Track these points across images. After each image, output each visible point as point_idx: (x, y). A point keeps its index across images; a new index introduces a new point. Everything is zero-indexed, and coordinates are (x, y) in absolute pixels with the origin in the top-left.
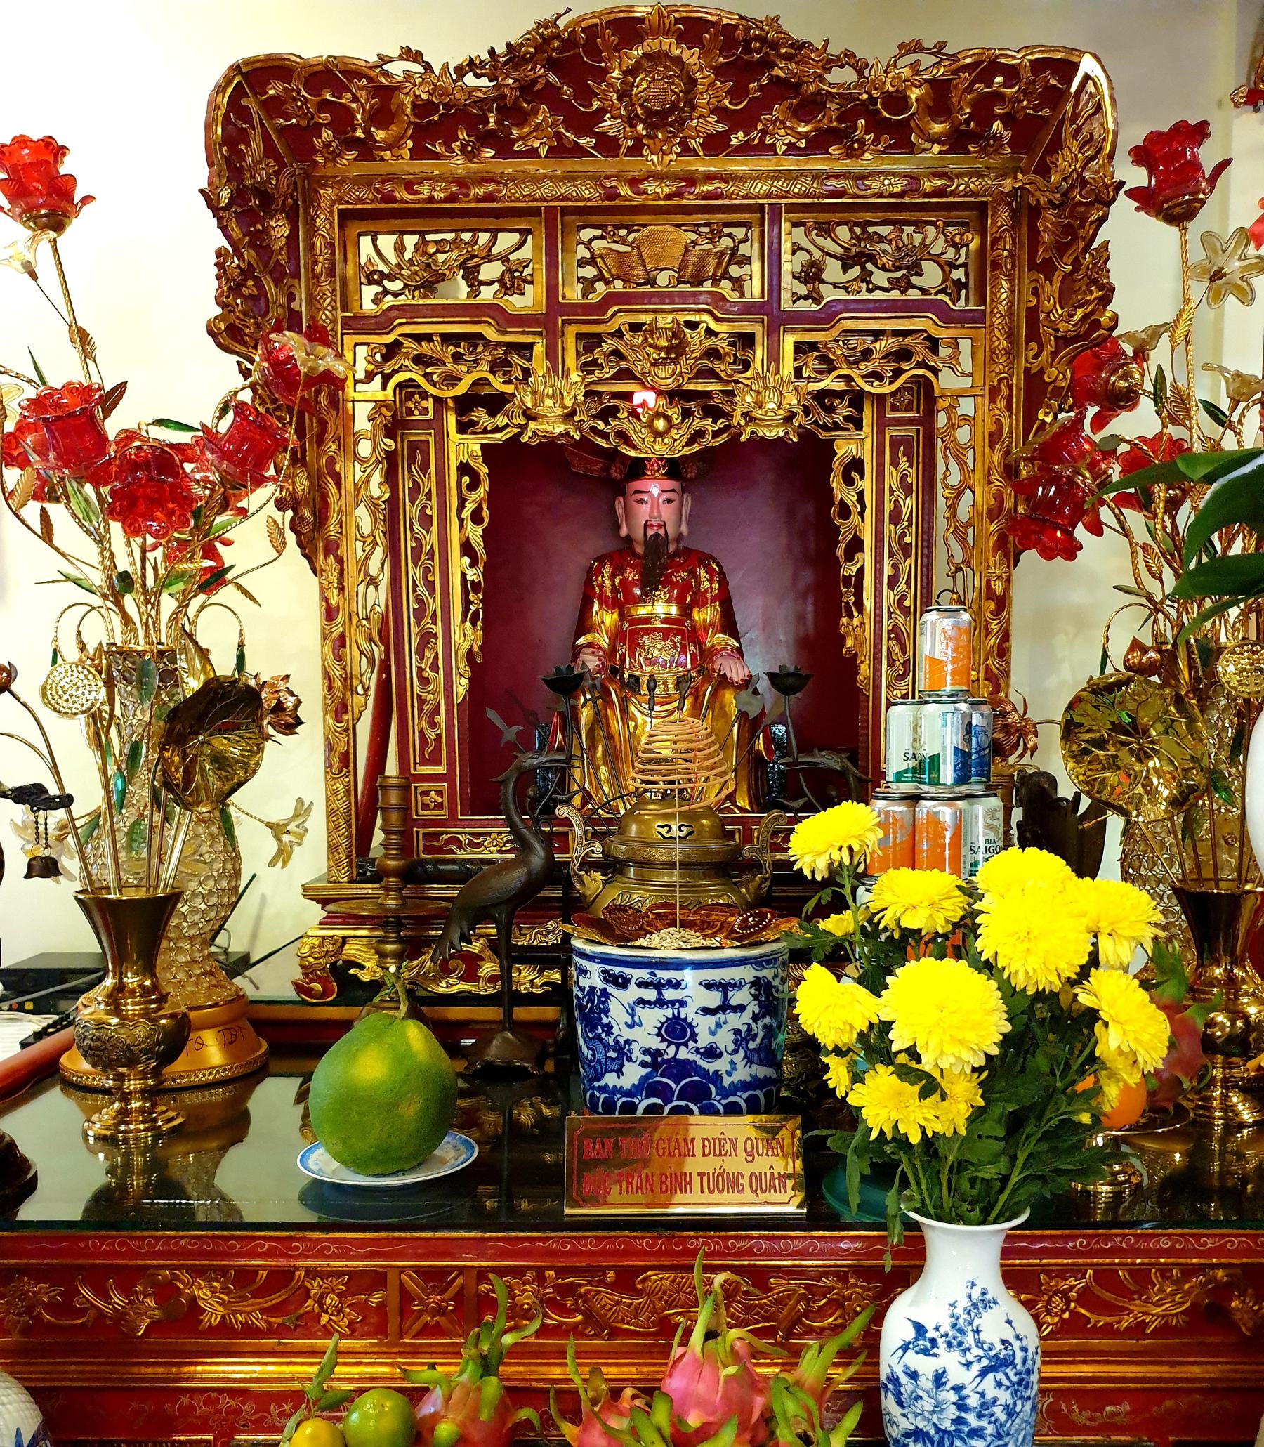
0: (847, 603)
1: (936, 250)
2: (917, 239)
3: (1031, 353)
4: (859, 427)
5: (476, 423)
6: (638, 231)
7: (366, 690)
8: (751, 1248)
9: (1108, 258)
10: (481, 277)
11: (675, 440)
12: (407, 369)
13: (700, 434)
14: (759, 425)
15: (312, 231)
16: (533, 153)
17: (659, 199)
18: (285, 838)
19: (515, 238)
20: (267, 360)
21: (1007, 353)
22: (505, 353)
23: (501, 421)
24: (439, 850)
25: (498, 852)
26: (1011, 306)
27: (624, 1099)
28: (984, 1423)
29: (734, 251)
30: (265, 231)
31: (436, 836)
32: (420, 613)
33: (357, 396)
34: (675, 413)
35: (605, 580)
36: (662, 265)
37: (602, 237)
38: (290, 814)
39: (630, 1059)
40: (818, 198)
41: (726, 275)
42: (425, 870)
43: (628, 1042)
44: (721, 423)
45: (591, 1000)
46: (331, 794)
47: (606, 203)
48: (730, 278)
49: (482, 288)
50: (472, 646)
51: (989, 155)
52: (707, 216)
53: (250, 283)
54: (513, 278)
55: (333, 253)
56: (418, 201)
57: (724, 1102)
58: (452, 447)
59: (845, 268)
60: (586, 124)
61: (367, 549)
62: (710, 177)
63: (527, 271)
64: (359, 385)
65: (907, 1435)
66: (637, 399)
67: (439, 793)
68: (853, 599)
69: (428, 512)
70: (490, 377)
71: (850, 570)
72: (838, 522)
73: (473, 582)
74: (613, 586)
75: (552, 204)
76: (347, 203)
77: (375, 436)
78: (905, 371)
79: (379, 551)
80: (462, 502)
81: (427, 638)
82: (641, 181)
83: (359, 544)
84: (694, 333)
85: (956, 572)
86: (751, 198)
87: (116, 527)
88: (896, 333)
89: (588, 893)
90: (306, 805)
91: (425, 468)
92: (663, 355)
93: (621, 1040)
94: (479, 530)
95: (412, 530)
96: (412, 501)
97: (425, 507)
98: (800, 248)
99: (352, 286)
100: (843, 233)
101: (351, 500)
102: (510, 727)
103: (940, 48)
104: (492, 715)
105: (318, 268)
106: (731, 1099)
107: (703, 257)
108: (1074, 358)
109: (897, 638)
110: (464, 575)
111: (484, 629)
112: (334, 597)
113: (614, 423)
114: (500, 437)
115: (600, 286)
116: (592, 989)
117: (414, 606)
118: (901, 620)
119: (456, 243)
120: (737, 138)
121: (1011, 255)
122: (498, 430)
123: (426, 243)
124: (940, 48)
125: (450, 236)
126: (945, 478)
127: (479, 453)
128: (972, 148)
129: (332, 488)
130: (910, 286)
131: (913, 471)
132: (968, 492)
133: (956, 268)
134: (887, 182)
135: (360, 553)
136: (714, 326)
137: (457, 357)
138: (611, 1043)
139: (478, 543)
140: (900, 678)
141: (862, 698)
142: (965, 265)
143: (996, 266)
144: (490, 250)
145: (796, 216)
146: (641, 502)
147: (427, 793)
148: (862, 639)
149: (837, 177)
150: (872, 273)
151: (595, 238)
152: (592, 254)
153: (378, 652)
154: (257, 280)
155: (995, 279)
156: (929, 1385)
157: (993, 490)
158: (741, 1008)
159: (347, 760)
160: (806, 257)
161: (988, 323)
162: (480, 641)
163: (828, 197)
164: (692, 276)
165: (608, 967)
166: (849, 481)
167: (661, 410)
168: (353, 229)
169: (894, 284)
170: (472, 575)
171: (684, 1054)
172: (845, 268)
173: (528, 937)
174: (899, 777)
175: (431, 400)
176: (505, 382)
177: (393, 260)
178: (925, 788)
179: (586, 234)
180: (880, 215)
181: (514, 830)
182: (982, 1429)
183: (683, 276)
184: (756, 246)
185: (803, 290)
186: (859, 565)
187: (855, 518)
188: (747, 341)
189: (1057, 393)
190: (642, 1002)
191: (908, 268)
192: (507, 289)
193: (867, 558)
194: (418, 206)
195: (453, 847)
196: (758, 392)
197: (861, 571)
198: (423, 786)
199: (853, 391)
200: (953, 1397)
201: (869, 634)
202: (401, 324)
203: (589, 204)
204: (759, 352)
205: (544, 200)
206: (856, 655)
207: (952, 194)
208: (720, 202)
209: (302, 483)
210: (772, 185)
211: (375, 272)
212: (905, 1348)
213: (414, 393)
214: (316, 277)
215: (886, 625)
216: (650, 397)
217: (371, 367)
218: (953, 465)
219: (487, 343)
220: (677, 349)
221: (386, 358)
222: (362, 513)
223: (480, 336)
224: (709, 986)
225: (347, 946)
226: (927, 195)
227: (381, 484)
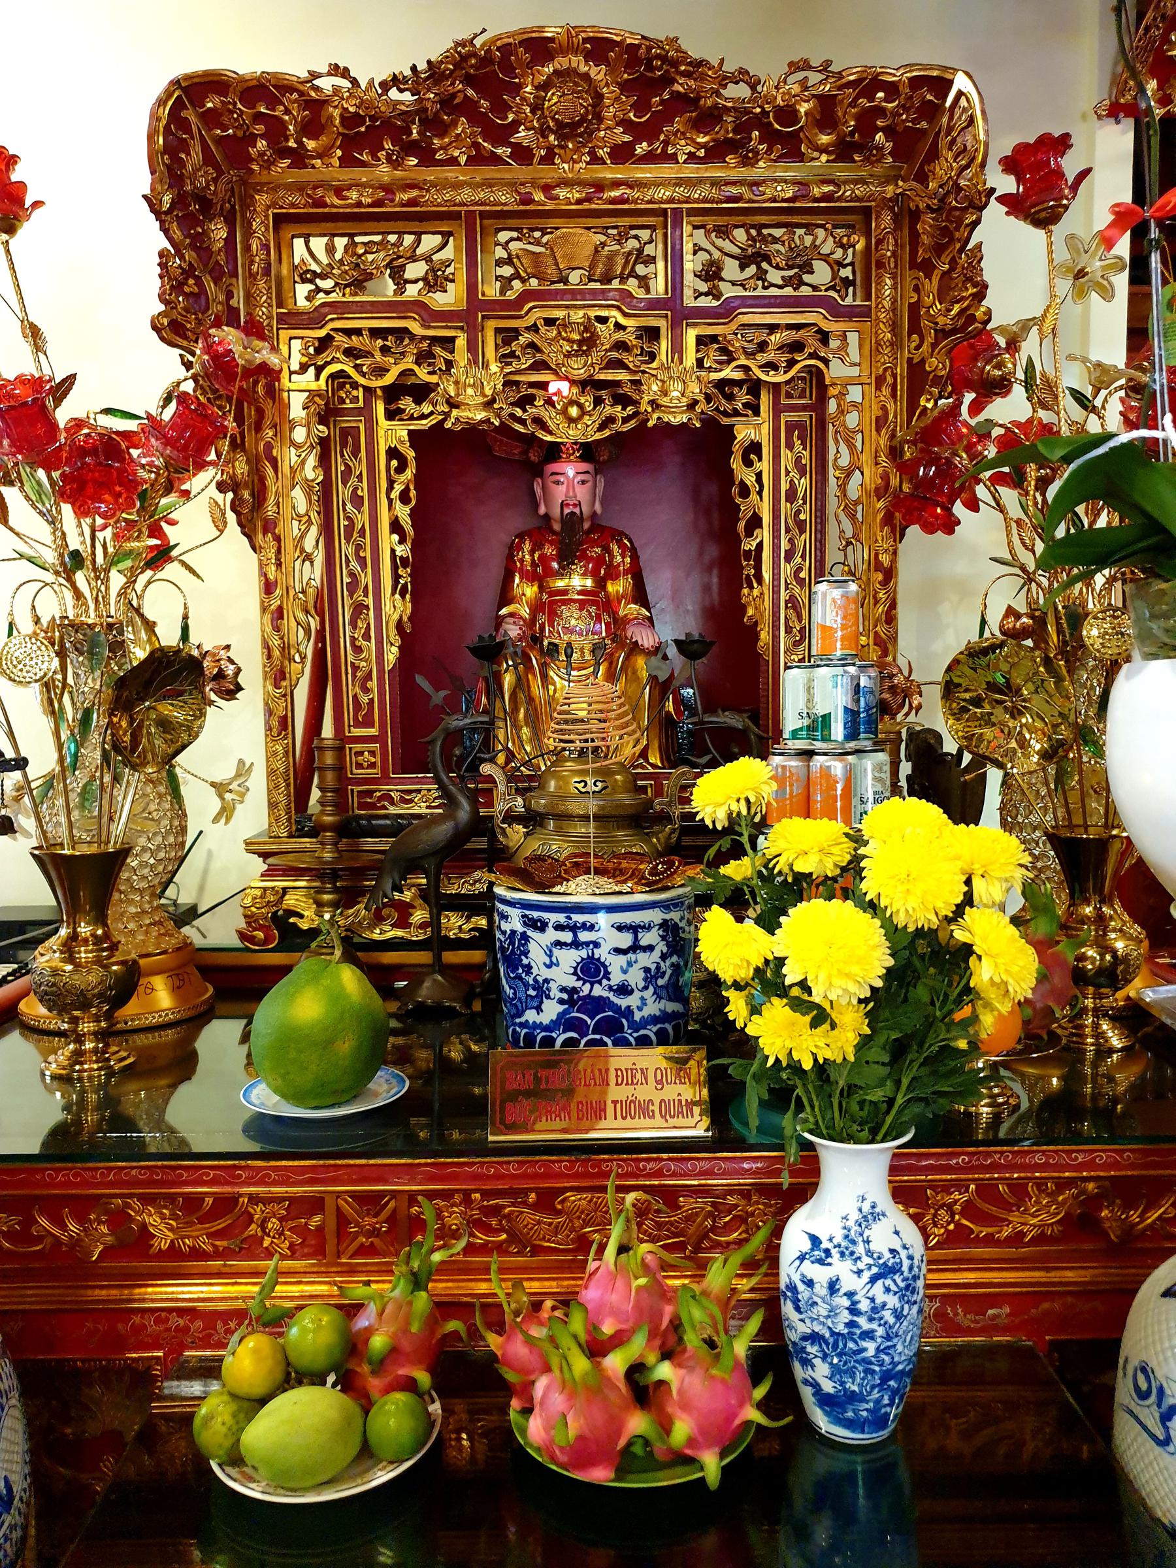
0: (748, 575)
1: (825, 250)
2: (808, 240)
3: (913, 345)
4: (757, 413)
5: (404, 411)
6: (551, 233)
7: (303, 658)
8: (661, 1169)
9: (981, 258)
10: (406, 276)
11: (588, 426)
13: (611, 420)
14: (664, 412)
15: (249, 233)
16: (453, 161)
17: (571, 204)
18: (228, 796)
19: (437, 239)
20: (208, 353)
21: (892, 344)
22: (429, 346)
23: (426, 408)
24: (373, 806)
25: (428, 807)
26: (894, 302)
27: (544, 1034)
28: (874, 1326)
29: (640, 251)
30: (205, 233)
31: (370, 793)
32: (353, 587)
33: (292, 386)
34: (587, 401)
35: (526, 554)
36: (574, 265)
37: (518, 239)
38: (232, 774)
39: (548, 997)
40: (717, 203)
41: (633, 274)
42: (359, 825)
43: (546, 981)
44: (630, 410)
45: (512, 943)
46: (271, 755)
47: (522, 207)
48: (637, 277)
49: (407, 286)
50: (401, 617)
51: (872, 163)
53: (191, 281)
54: (436, 277)
55: (269, 254)
56: (348, 206)
57: (635, 1035)
58: (381, 433)
59: (743, 267)
60: (501, 135)
61: (303, 528)
62: (616, 184)
63: (450, 270)
64: (294, 377)
65: (804, 1338)
66: (552, 388)
67: (373, 753)
68: (753, 571)
69: (359, 493)
70: (416, 368)
71: (750, 545)
72: (738, 500)
73: (401, 558)
74: (533, 560)
75: (471, 208)
76: (282, 207)
77: (309, 423)
79: (314, 530)
80: (390, 488)
81: (359, 609)
83: (295, 523)
84: (603, 327)
85: (847, 546)
87: (67, 509)
88: (790, 327)
89: (511, 844)
90: (247, 766)
91: (356, 452)
93: (540, 979)
94: (407, 509)
95: (344, 510)
96: (345, 483)
97: (356, 489)
98: (701, 249)
99: (286, 285)
100: (740, 234)
101: (288, 483)
102: (437, 690)
103: (825, 67)
104: (420, 680)
105: (255, 267)
106: (642, 1032)
107: (611, 258)
108: (951, 350)
110: (393, 551)
111: (413, 601)
114: (425, 424)
115: (516, 284)
116: (513, 932)
117: (347, 580)
119: (383, 244)
120: (642, 148)
122: (423, 417)
123: (355, 244)
124: (825, 67)
125: (378, 238)
126: (836, 459)
127: (407, 438)
129: (270, 471)
130: (802, 283)
131: (806, 453)
133: (845, 266)
134: (779, 188)
135: (296, 532)
136: (622, 321)
137: (385, 350)
138: (531, 982)
140: (797, 644)
141: (762, 663)
142: (852, 264)
143: (880, 265)
144: (414, 251)
145: (697, 220)
146: (558, 483)
147: (361, 753)
148: (762, 608)
149: (734, 183)
150: (767, 272)
151: (512, 239)
152: (509, 255)
153: (314, 623)
154: (198, 279)
155: (880, 277)
157: (880, 470)
158: (651, 948)
159: (285, 723)
160: (705, 256)
161: (873, 317)
162: (408, 612)
164: (601, 274)
165: (527, 912)
166: (748, 463)
167: (574, 398)
168: (288, 231)
169: (787, 282)
170: (401, 551)
171: (598, 991)
172: (743, 267)
173: (456, 886)
174: (795, 735)
175: (361, 389)
176: (429, 373)
177: (325, 260)
178: (819, 745)
179: (503, 236)
181: (442, 787)
182: (873, 1331)
183: (594, 275)
184: (660, 246)
185: (703, 287)
186: (758, 541)
187: (754, 497)
188: (653, 334)
189: (937, 381)
190: (559, 944)
191: (800, 267)
193: (766, 533)
194: (348, 210)
196: (663, 382)
197: (760, 546)
198: (358, 747)
200: (846, 1302)
201: (768, 603)
202: (332, 320)
203: (505, 208)
206: (756, 623)
207: (839, 199)
208: (626, 206)
209: (241, 467)
210: (674, 191)
211: (308, 271)
212: (802, 1258)
213: (345, 383)
214: (252, 276)
216: (564, 387)
217: (305, 359)
218: (843, 448)
219: (412, 337)
220: (588, 342)
221: (319, 351)
222: (298, 494)
223: (406, 330)
224: (620, 928)
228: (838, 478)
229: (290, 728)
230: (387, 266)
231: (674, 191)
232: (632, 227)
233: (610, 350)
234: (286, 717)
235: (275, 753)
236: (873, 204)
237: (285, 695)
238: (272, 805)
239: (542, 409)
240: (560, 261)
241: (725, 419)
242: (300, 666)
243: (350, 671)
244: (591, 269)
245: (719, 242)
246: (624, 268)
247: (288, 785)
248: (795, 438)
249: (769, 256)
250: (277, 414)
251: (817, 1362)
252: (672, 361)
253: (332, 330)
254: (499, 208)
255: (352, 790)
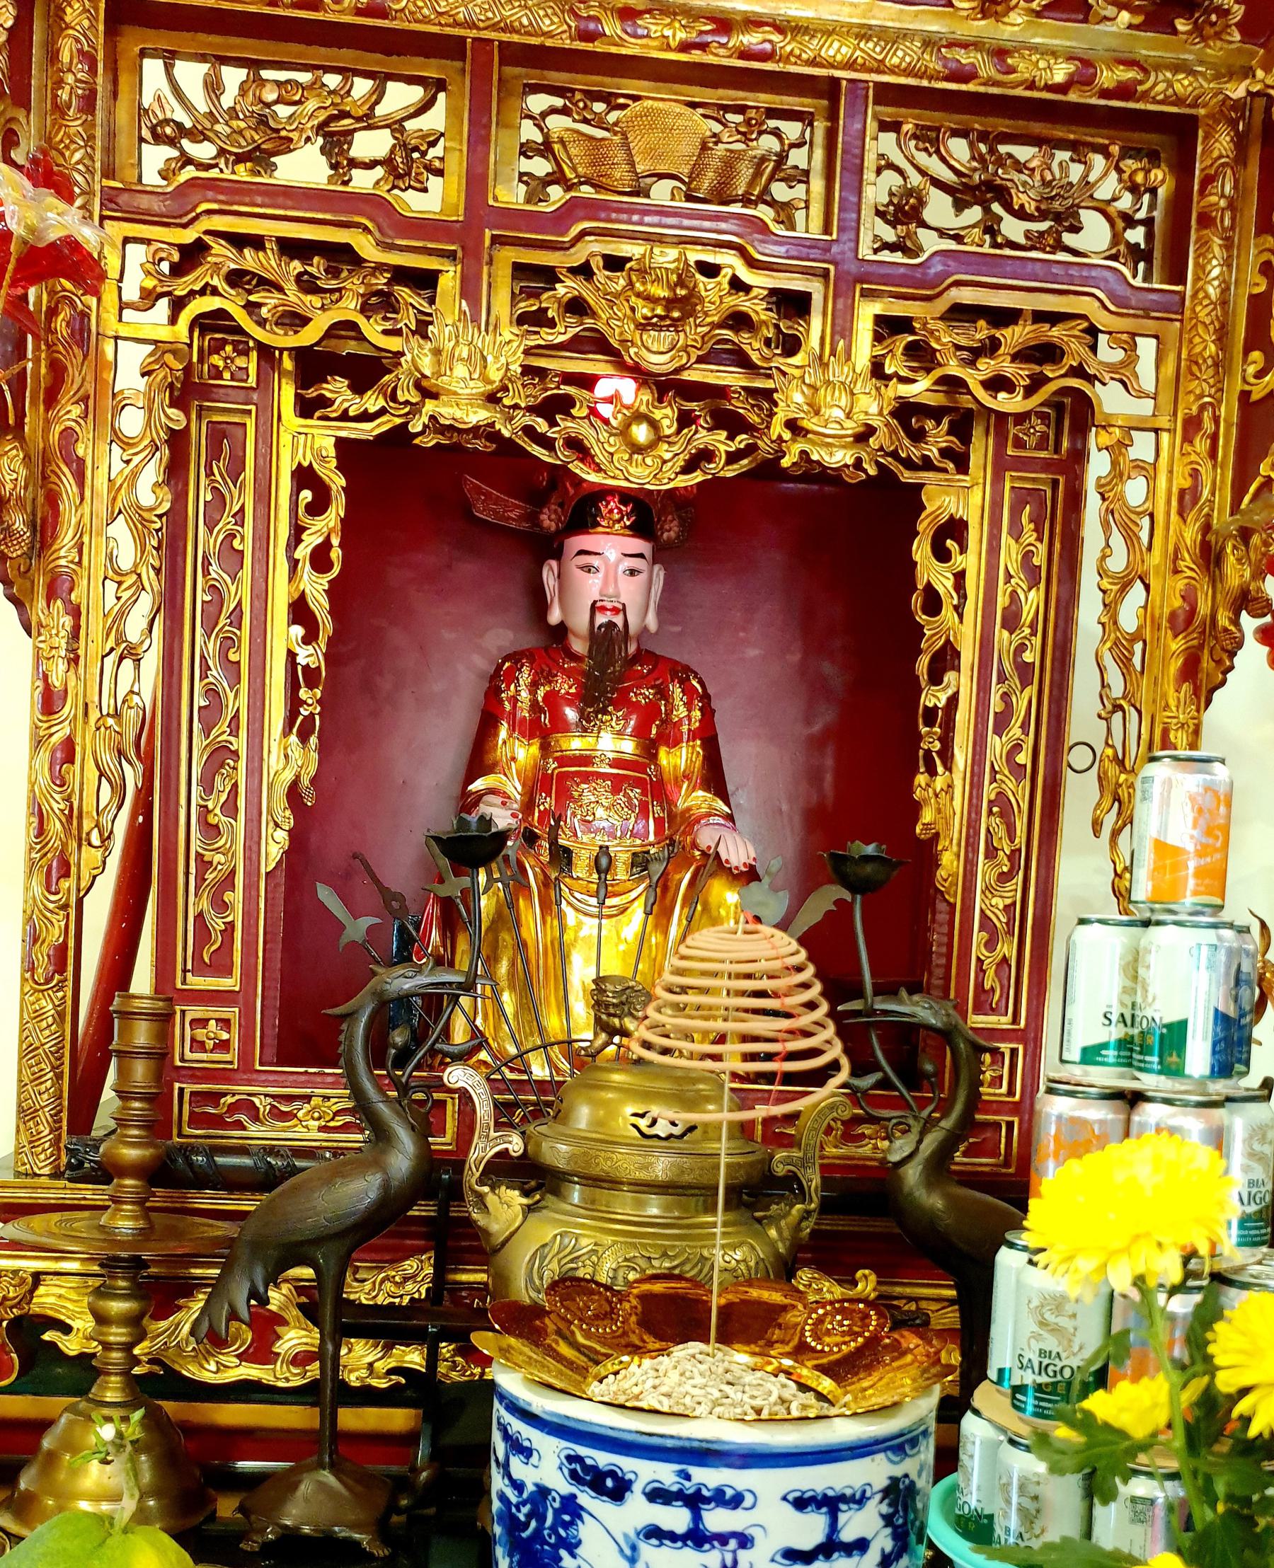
3: (1251, 370)
4: (963, 467)
6: (624, 107)
7: (106, 839)
10: (353, 153)
11: (665, 462)
12: (215, 292)
13: (705, 455)
14: (813, 443)
17: (668, 48)
19: (416, 93)
21: (1216, 365)
23: (373, 402)
24: (218, 1122)
25: (321, 1129)
26: (1225, 290)
29: (782, 158)
31: (215, 1097)
34: (666, 416)
36: (662, 169)
37: (564, 111)
40: (930, 78)
41: (765, 198)
42: (190, 1164)
44: (742, 440)
48: (772, 203)
49: (355, 172)
50: (298, 777)
52: (741, 94)
54: (409, 162)
58: (286, 439)
59: (959, 206)
61: (126, 595)
64: (127, 313)
66: (603, 388)
67: (225, 1023)
68: (937, 745)
69: (236, 544)
70: (361, 320)
71: (934, 698)
72: (921, 618)
73: (306, 668)
77: (151, 401)
78: (1051, 380)
79: (145, 603)
80: (297, 532)
81: (220, 756)
82: (640, 14)
83: (111, 587)
84: (710, 283)
85: (1113, 712)
86: (822, 66)
88: (1040, 317)
91: (236, 470)
92: (659, 311)
94: (324, 581)
95: (206, 573)
98: (891, 166)
99: (124, 141)
100: (959, 149)
101: (102, 508)
104: (325, 894)
107: (729, 164)
109: (1001, 815)
110: (291, 655)
111: (322, 750)
112: (58, 673)
113: (564, 423)
115: (555, 192)
117: (200, 701)
118: (1010, 785)
119: (316, 85)
121: (1232, 206)
122: (365, 417)
123: (262, 82)
125: (304, 77)
127: (332, 452)
128: (1182, 25)
131: (1042, 548)
132: (1138, 585)
134: (1042, 64)
135: (110, 600)
136: (747, 276)
137: (307, 285)
139: (320, 604)
140: (1004, 878)
141: (941, 906)
142: (1148, 223)
143: (1206, 220)
144: (372, 108)
145: (888, 112)
147: (203, 1023)
148: (949, 812)
149: (965, 45)
150: (1001, 219)
151: (553, 111)
153: (132, 777)
155: (1204, 244)
157: (1181, 584)
161: (1187, 313)
162: (312, 769)
163: (947, 79)
164: (712, 190)
166: (942, 555)
167: (643, 409)
169: (1035, 241)
170: (308, 656)
172: (959, 206)
173: (368, 1286)
175: (254, 355)
176: (386, 332)
177: (202, 105)
179: (538, 103)
180: (1020, 126)
181: (357, 1093)
183: (696, 190)
184: (819, 154)
185: (889, 235)
186: (950, 692)
187: (948, 613)
191: (1058, 218)
192: (399, 177)
193: (965, 679)
195: (243, 1118)
196: (814, 388)
197: (953, 701)
198: (195, 1012)
199: (955, 409)
201: (959, 802)
202: (209, 212)
203: (549, 43)
204: (816, 322)
205: (473, 26)
206: (937, 835)
207: (1145, 96)
208: (768, 66)
210: (857, 47)
211: (167, 121)
213: (225, 342)
215: (989, 792)
216: (627, 388)
217: (150, 283)
218: (1117, 540)
219: (356, 260)
221: (178, 270)
222: (120, 529)
225: (41, 1290)
226: (1105, 94)
227: (157, 485)
228: (1104, 592)
229: (70, 968)
230: (320, 128)
231: (857, 47)
232: (772, 113)
233: (721, 325)
234: (64, 947)
235: (38, 1015)
236: (1202, 112)
237: (65, 907)
238: (25, 1113)
239: (585, 423)
240: (637, 159)
241: (907, 474)
242: (99, 854)
243: (193, 870)
244: (692, 179)
245: (921, 157)
246: (751, 184)
247: (59, 1076)
248: (1025, 519)
249: (1007, 189)
250: (90, 378)
252: (833, 353)
253: (207, 232)
254: (535, 41)
255: (181, 1090)
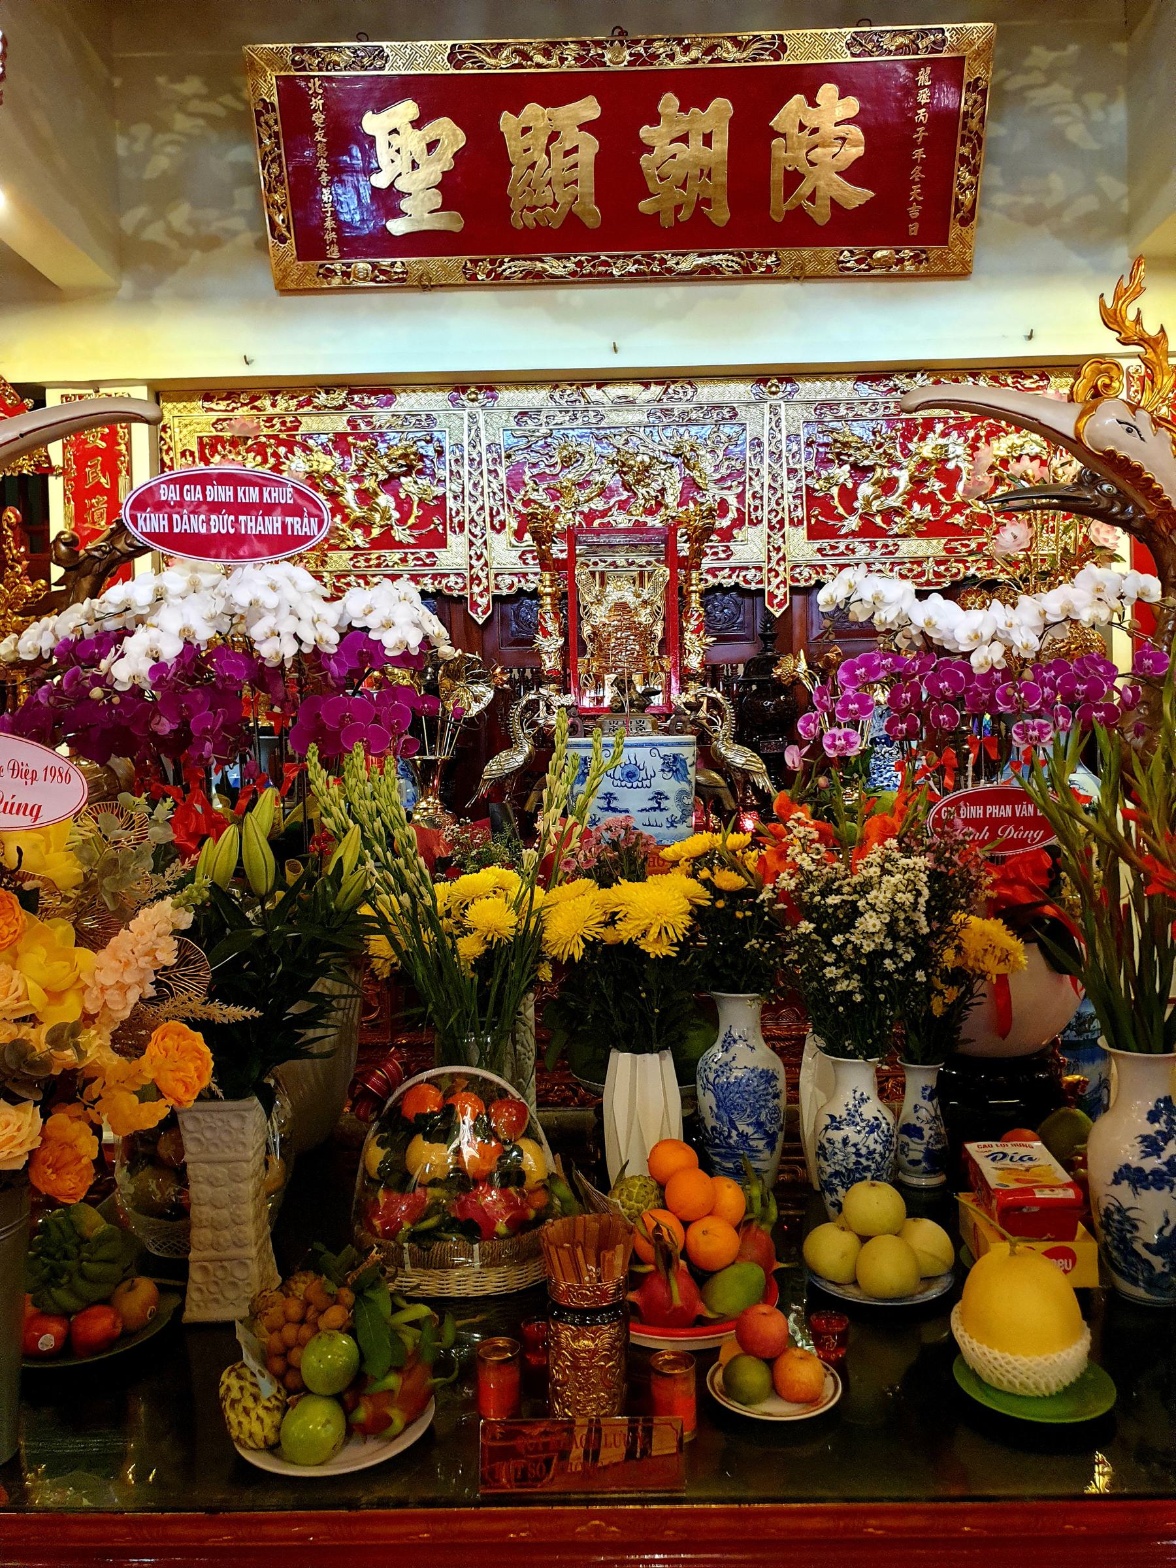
28: (870, 1163)
65: (831, 1175)
156: (840, 1146)
200: (854, 1150)
212: (827, 1128)
251: (839, 1188)
